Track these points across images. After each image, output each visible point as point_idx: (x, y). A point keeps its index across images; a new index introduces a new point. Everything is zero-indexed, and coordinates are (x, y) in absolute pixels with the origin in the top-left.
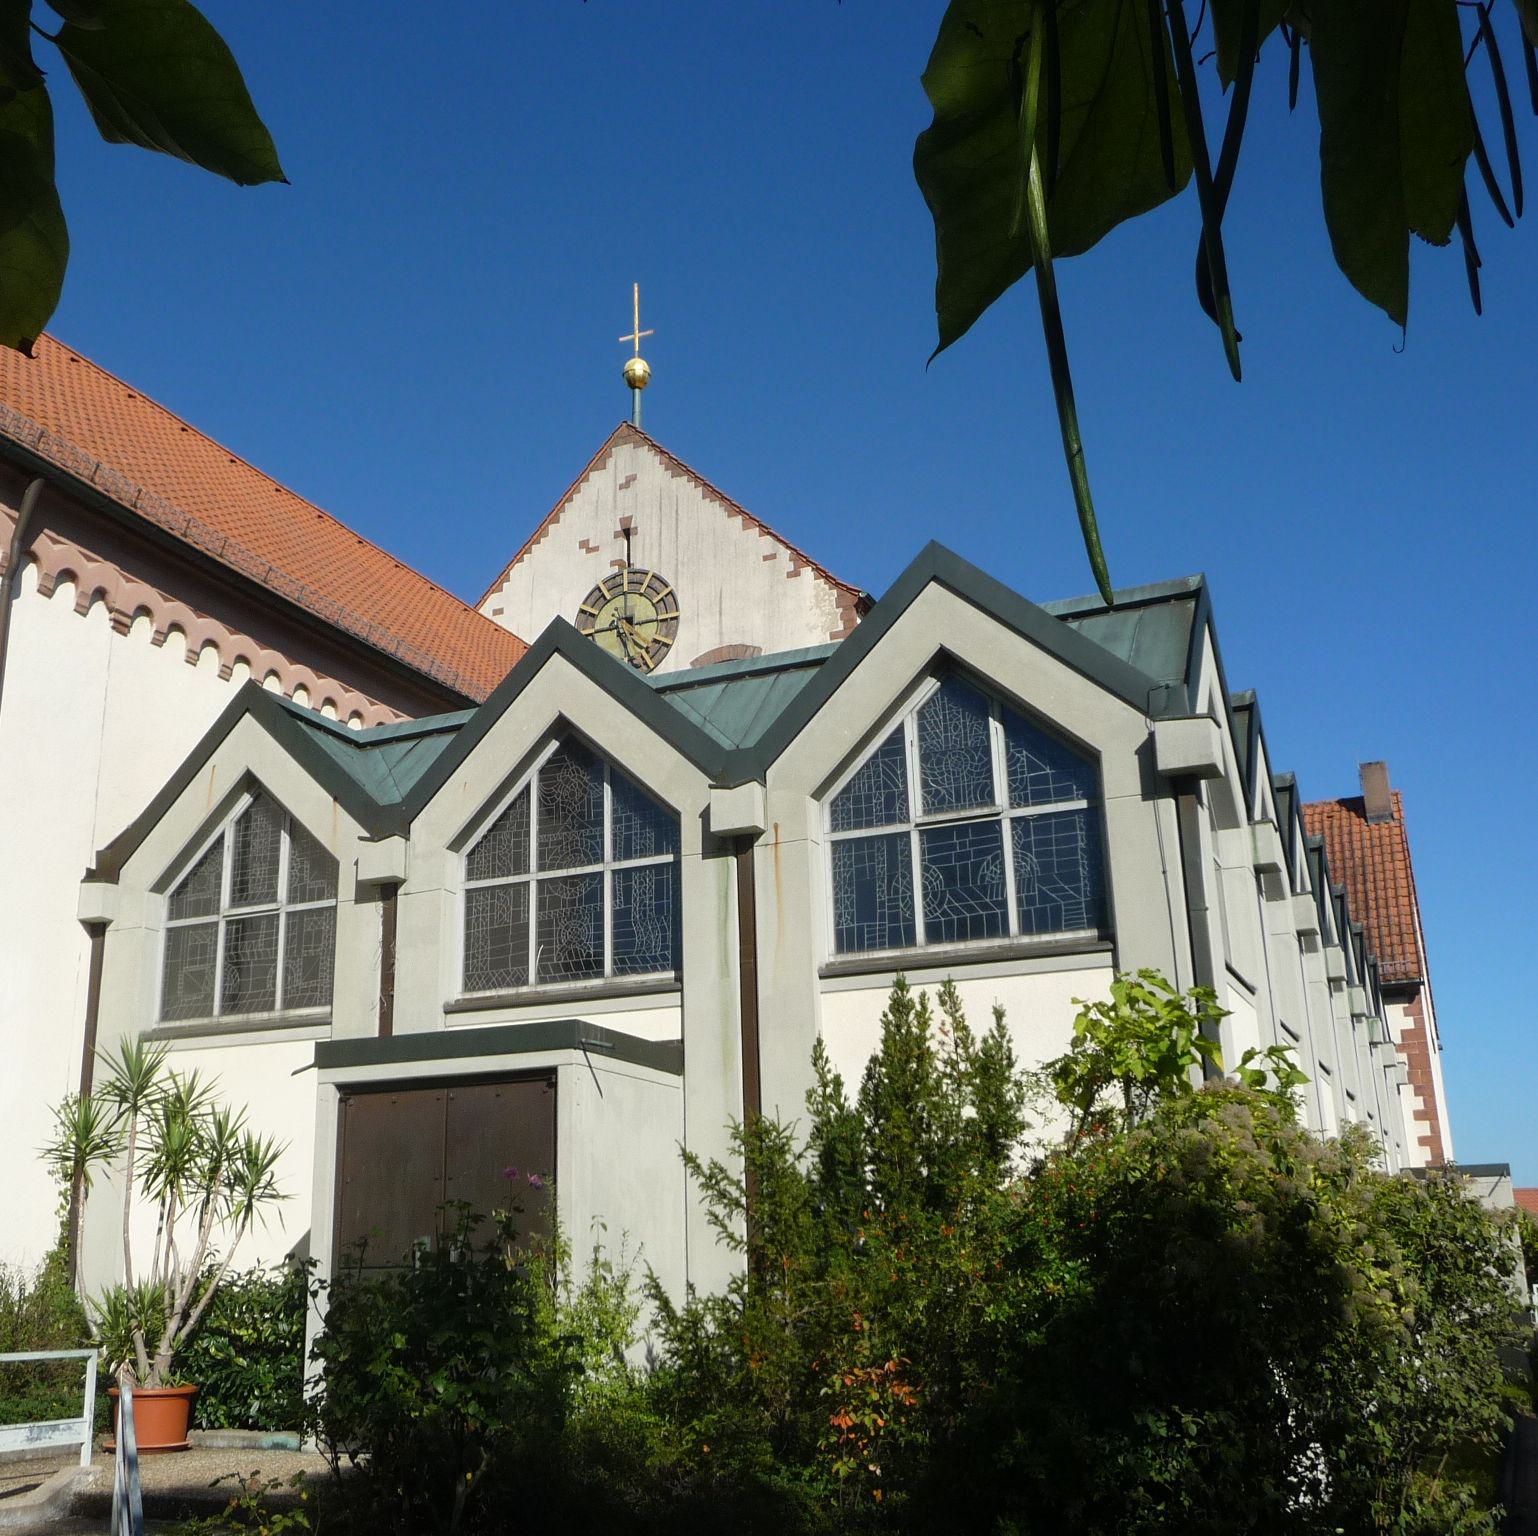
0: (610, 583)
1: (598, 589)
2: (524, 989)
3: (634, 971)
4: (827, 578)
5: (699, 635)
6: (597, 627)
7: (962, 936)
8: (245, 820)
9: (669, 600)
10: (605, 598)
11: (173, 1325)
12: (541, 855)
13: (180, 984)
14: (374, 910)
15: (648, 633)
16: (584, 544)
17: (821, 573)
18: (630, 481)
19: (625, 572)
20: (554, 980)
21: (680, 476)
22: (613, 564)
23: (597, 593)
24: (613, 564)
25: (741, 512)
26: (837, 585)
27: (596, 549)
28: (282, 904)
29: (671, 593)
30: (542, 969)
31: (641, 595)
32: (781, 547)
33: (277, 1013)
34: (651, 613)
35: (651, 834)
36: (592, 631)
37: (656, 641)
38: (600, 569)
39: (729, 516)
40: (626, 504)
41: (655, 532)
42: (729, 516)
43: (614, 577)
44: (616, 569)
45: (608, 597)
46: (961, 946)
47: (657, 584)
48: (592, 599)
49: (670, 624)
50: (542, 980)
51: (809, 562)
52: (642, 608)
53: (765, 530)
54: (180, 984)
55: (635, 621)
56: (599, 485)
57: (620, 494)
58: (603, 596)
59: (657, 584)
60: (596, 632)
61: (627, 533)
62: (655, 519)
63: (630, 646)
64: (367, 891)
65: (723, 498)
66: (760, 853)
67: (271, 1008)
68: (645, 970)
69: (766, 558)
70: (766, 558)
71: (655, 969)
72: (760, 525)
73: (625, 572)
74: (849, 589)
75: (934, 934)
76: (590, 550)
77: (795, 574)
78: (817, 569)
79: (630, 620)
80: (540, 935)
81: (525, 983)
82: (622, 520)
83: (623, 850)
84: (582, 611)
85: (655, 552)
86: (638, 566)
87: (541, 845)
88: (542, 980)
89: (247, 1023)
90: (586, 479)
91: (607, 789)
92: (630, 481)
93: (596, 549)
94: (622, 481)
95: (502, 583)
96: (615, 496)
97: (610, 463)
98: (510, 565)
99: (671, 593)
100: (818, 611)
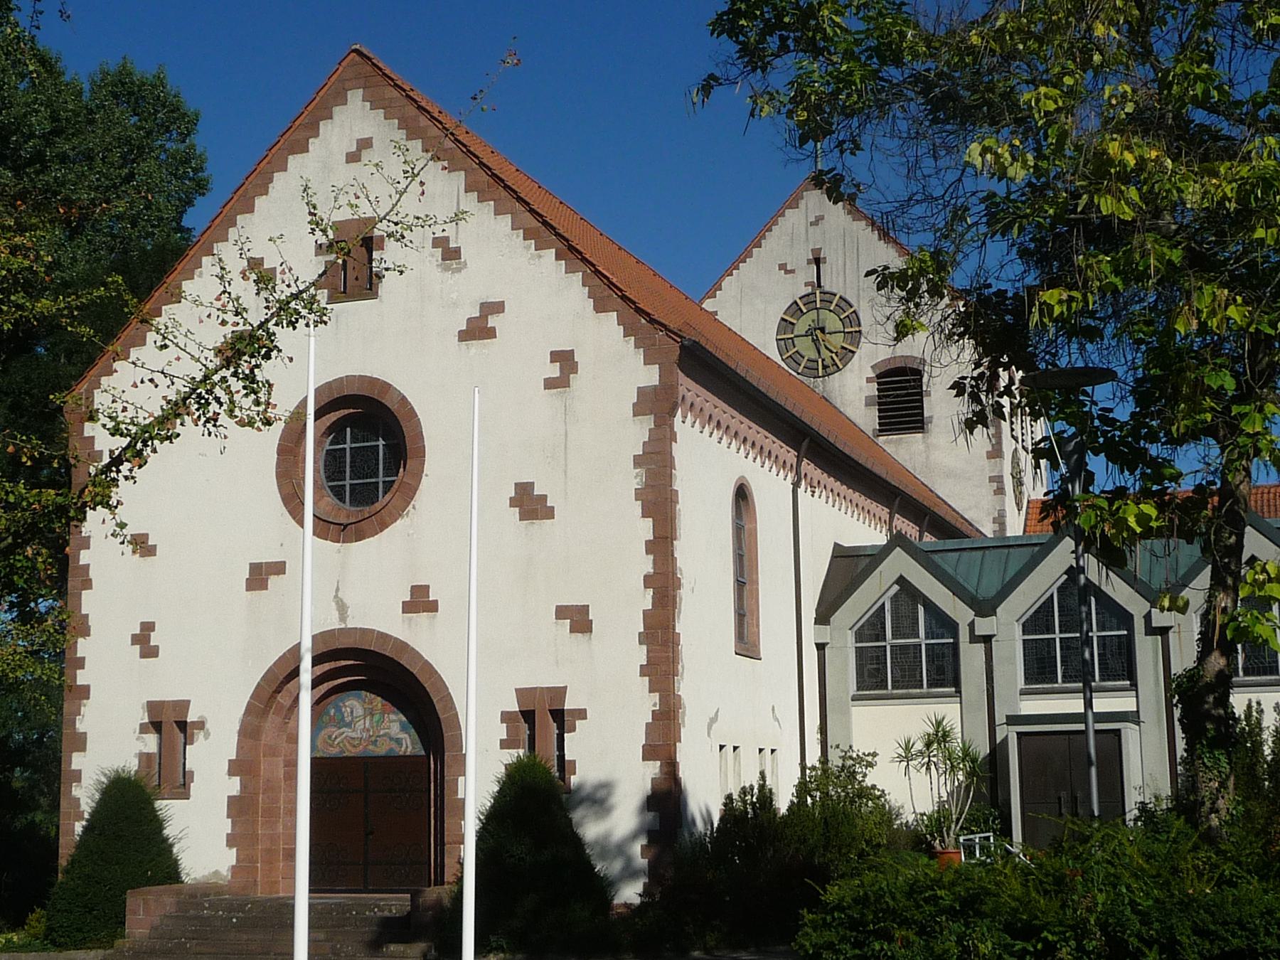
0: (805, 300)
1: (796, 302)
2: (1056, 685)
3: (1109, 680)
6: (796, 333)
7: (1259, 674)
8: (895, 598)
10: (802, 311)
11: (953, 826)
12: (1060, 626)
13: (866, 674)
14: (980, 648)
15: (837, 341)
16: (782, 267)
18: (818, 220)
19: (818, 292)
20: (1069, 682)
21: (859, 220)
22: (807, 284)
23: (795, 305)
24: (807, 284)
27: (792, 271)
28: (922, 639)
29: (854, 312)
30: (1064, 676)
31: (830, 311)
33: (925, 690)
34: (839, 326)
35: (1114, 621)
38: (797, 287)
40: (816, 238)
41: (840, 262)
43: (808, 295)
44: (809, 290)
45: (805, 311)
46: (1259, 678)
47: (843, 304)
48: (791, 311)
50: (1064, 682)
52: (832, 322)
54: (866, 674)
56: (793, 220)
57: (811, 229)
58: (800, 309)
59: (843, 304)
60: (796, 336)
61: (818, 261)
62: (840, 252)
63: (823, 350)
64: (974, 639)
66: (1171, 634)
67: (921, 686)
68: (1115, 680)
71: (1119, 680)
73: (818, 292)
75: (1246, 673)
76: (787, 272)
79: (822, 330)
80: (1062, 661)
81: (1057, 682)
83: (1102, 627)
84: (783, 319)
85: (841, 279)
86: (827, 289)
87: (1060, 621)
88: (1064, 682)
89: (909, 694)
90: (783, 215)
91: (1093, 599)
92: (818, 220)
93: (792, 271)
95: (716, 290)
96: (807, 231)
97: (802, 203)
98: (722, 278)
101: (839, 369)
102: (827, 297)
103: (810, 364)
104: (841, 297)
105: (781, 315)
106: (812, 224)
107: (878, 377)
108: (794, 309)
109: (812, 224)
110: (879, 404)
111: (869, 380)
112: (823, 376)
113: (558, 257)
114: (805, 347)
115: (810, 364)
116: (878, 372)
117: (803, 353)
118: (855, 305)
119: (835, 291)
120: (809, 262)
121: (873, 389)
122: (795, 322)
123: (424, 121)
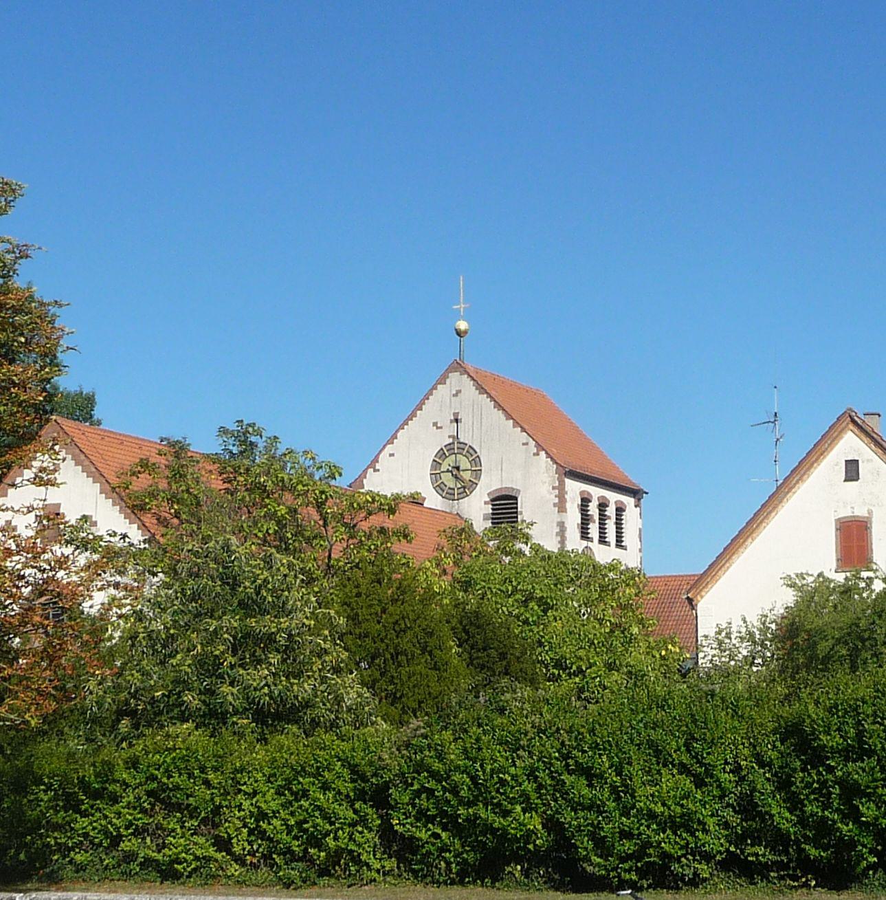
1: (442, 449)
4: (552, 459)
5: (491, 480)
9: (476, 461)
16: (435, 424)
17: (548, 455)
18: (459, 392)
22: (450, 437)
24: (450, 437)
25: (513, 419)
26: (556, 463)
27: (441, 428)
32: (531, 439)
36: (438, 472)
37: (470, 481)
39: (507, 419)
42: (507, 419)
43: (450, 444)
44: (451, 440)
47: (471, 451)
48: (439, 455)
49: (477, 473)
51: (543, 450)
52: (464, 463)
53: (523, 430)
55: (461, 468)
58: (444, 454)
59: (471, 451)
61: (457, 421)
62: (470, 416)
65: (504, 410)
69: (524, 444)
70: (524, 444)
72: (521, 427)
74: (561, 466)
76: (438, 428)
77: (537, 454)
78: (547, 453)
79: (458, 468)
82: (454, 414)
84: (434, 460)
86: (462, 440)
92: (459, 392)
93: (441, 428)
94: (454, 392)
97: (448, 381)
98: (397, 431)
99: (478, 456)
100: (546, 475)
101: (467, 496)
102: (462, 446)
103: (450, 491)
104: (470, 446)
105: (433, 457)
106: (454, 395)
107: (493, 500)
108: (442, 454)
109: (454, 395)
110: (493, 519)
111: (486, 503)
112: (458, 500)
113: (139, 529)
114: (448, 479)
115: (450, 491)
116: (492, 497)
117: (446, 483)
118: (479, 454)
119: (466, 442)
120: (451, 422)
121: (489, 509)
122: (440, 462)
123: (83, 457)
